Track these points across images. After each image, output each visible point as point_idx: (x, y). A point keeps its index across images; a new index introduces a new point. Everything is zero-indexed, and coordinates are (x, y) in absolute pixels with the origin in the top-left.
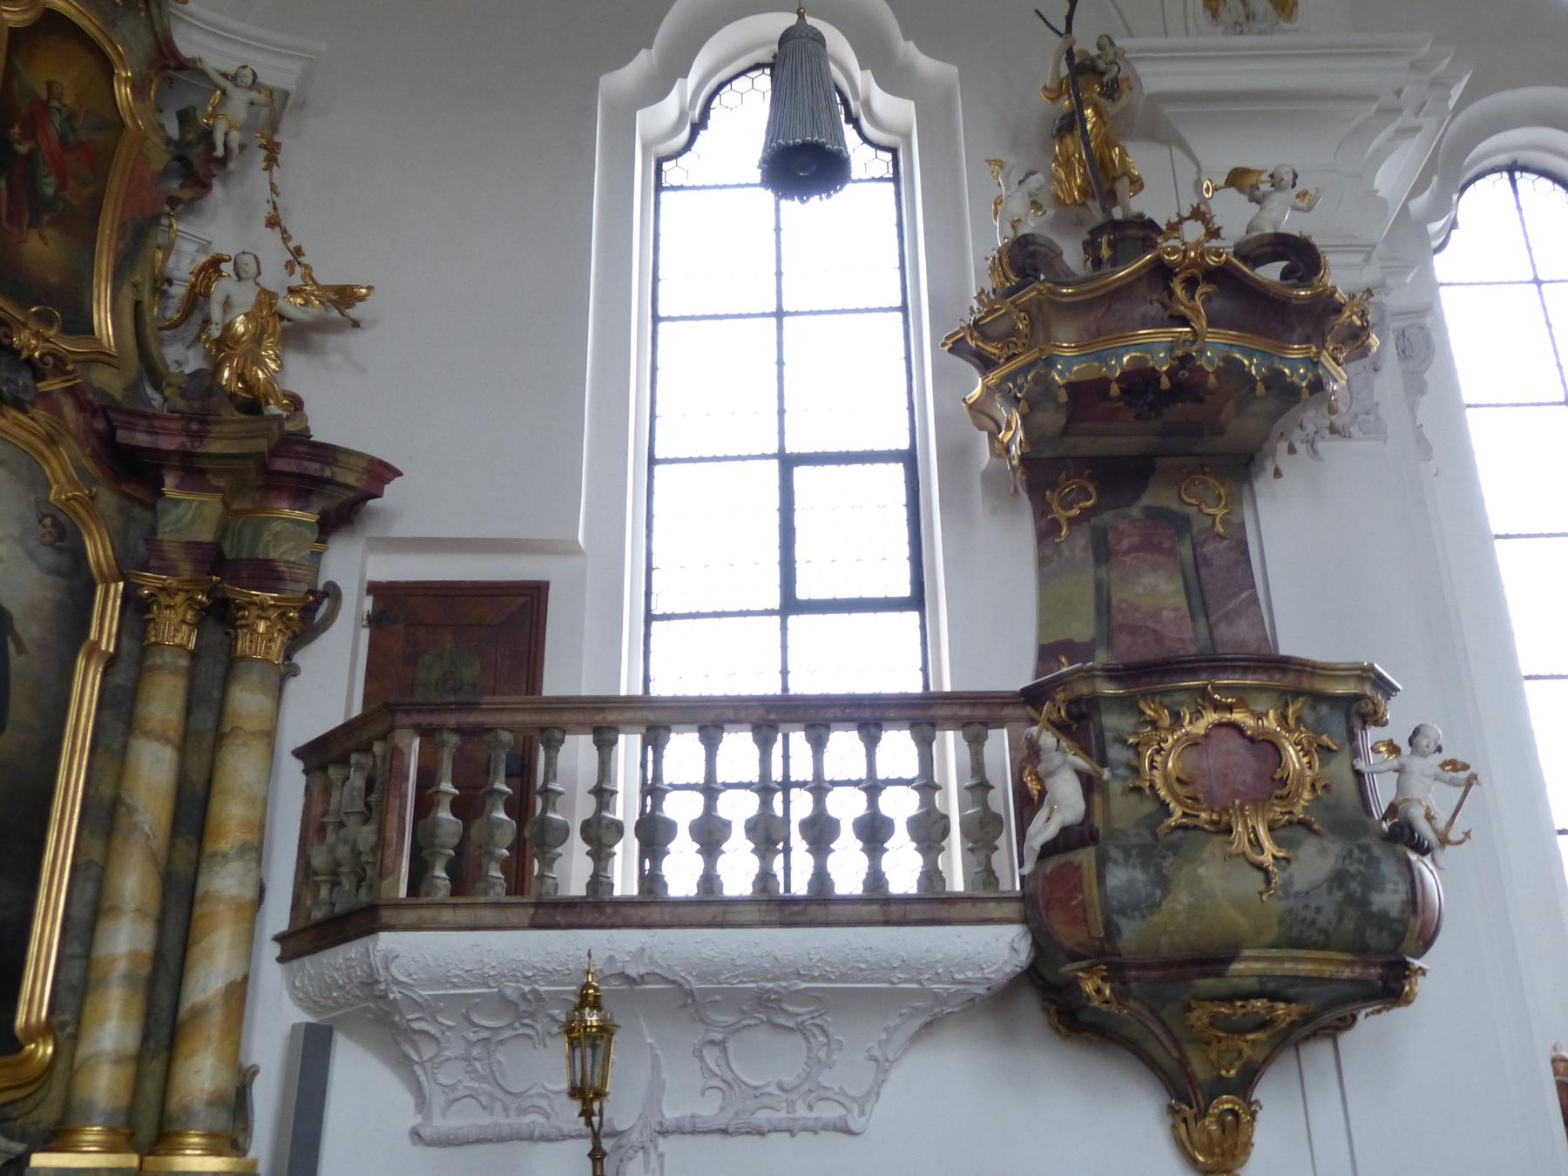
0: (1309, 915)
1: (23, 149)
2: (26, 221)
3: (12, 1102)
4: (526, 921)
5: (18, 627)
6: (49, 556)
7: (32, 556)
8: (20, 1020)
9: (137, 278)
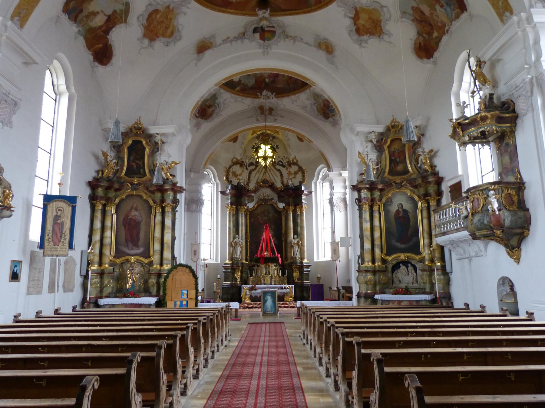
0: (477, 226)
1: (393, 158)
5: (409, 211)
6: (410, 202)
7: (408, 202)
8: (421, 251)
9: (413, 161)
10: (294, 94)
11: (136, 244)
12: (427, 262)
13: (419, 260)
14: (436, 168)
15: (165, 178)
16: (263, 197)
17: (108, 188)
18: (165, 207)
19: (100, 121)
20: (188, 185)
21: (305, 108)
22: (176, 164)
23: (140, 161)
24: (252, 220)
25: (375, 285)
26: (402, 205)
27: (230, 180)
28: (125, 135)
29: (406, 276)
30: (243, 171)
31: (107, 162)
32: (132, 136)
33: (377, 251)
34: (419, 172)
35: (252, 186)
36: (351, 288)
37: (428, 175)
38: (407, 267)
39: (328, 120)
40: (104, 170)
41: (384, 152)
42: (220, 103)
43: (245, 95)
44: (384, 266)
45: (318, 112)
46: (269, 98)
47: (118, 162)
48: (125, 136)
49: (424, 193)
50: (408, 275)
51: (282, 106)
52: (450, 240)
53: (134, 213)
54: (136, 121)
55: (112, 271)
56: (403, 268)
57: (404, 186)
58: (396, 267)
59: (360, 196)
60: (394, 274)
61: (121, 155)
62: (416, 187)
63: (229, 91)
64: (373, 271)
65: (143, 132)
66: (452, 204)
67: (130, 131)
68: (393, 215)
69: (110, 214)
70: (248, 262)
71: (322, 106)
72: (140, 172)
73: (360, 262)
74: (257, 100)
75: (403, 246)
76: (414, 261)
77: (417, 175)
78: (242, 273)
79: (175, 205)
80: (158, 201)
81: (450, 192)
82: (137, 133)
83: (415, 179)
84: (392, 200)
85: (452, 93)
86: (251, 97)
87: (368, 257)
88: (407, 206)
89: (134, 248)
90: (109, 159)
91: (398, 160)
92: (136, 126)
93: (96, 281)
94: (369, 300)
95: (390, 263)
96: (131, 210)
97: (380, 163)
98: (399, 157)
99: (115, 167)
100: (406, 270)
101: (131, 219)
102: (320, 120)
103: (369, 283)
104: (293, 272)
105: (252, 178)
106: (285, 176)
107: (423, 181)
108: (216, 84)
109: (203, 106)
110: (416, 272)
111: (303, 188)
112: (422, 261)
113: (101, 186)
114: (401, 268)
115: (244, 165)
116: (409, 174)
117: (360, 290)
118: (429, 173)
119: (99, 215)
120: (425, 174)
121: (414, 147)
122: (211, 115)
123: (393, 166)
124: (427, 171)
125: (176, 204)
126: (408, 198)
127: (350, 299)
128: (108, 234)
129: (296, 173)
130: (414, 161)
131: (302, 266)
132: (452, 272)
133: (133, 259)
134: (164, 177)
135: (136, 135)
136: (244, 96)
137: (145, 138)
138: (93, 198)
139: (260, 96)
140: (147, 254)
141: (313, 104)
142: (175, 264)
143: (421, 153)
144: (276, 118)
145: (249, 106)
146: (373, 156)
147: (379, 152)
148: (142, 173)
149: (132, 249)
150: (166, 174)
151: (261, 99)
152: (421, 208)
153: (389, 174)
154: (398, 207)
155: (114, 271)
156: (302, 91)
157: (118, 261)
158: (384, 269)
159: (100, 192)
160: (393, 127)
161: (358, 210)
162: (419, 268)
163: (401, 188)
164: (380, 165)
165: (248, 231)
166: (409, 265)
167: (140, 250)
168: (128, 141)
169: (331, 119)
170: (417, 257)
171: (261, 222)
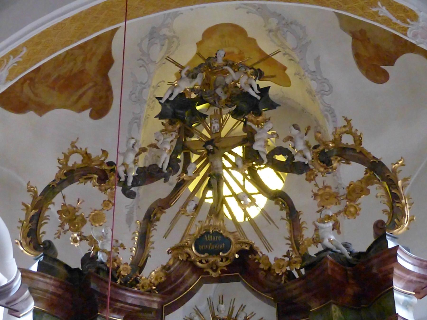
30: (107, 204)
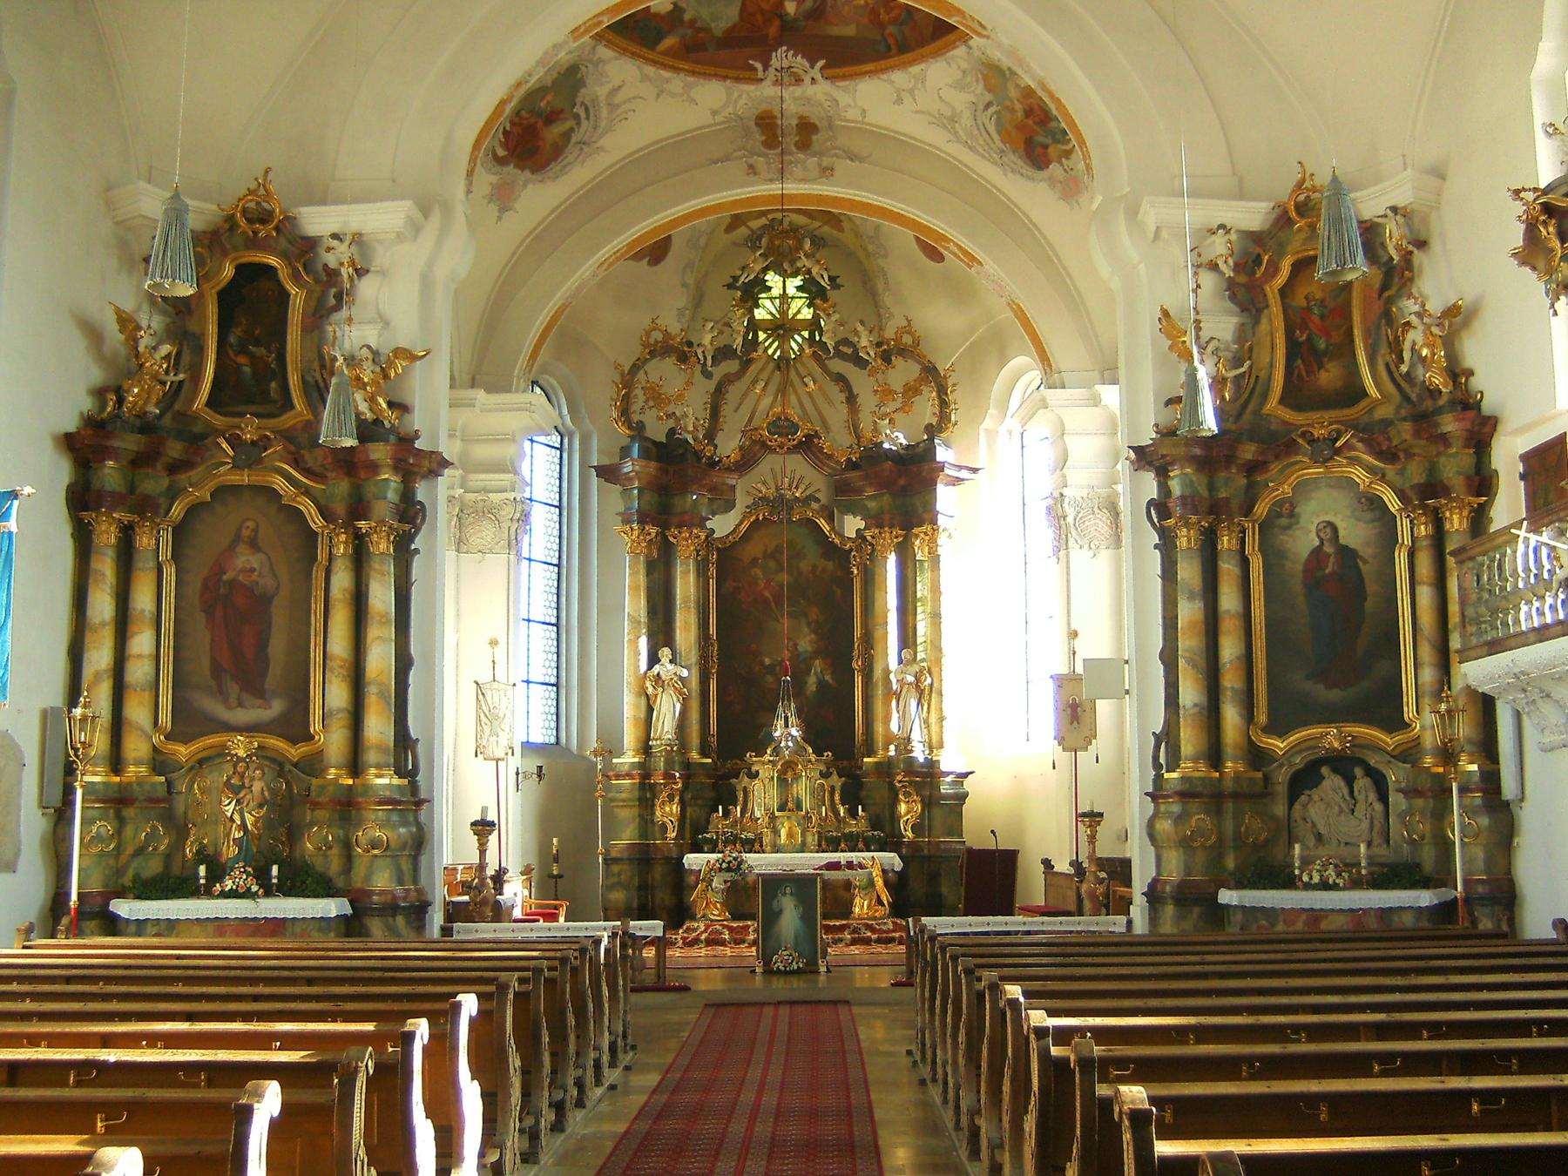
2: (1316, 368)
3: (1410, 748)
4: (1485, 652)
6: (1368, 516)
7: (1358, 519)
8: (1406, 716)
9: (1383, 352)
10: (903, 66)
11: (254, 686)
12: (1428, 761)
13: (1395, 753)
14: (1471, 378)
15: (369, 416)
16: (773, 490)
17: (141, 461)
18: (368, 534)
19: (109, 189)
20: (462, 440)
21: (948, 121)
22: (413, 358)
23: (270, 352)
24: (729, 585)
25: (1217, 851)
26: (1335, 529)
27: (636, 418)
28: (206, 242)
29: (1343, 817)
30: (689, 383)
31: (137, 355)
32: (235, 248)
33: (1231, 715)
34: (1406, 398)
35: (728, 446)
36: (1126, 864)
37: (1439, 411)
38: (1350, 781)
39: (1045, 174)
40: (125, 387)
41: (1266, 312)
42: (593, 101)
43: (698, 68)
44: (1259, 775)
45: (1005, 136)
46: (798, 81)
47: (179, 354)
48: (210, 248)
49: (1422, 481)
50: (1353, 811)
51: (852, 114)
52: (1516, 670)
53: (245, 559)
54: (253, 186)
55: (161, 792)
56: (1332, 782)
57: (1345, 451)
58: (1304, 780)
59: (1164, 489)
60: (1297, 806)
61: (193, 326)
62: (1389, 456)
63: (634, 55)
64: (1212, 796)
65: (277, 229)
66: (1520, 529)
67: (227, 226)
68: (1300, 567)
69: (152, 564)
70: (709, 761)
71: (1020, 115)
72: (265, 394)
73: (1162, 760)
74: (750, 88)
75: (1334, 695)
76: (1377, 758)
77: (1399, 407)
78: (682, 803)
79: (407, 527)
80: (340, 509)
81: (1523, 477)
82: (255, 233)
83: (1387, 423)
84: (1296, 510)
85: (1534, 75)
86: (725, 78)
87: (1190, 738)
88: (1355, 533)
89: (248, 699)
90: (145, 342)
91: (1322, 344)
92: (252, 205)
93: (102, 830)
94: (1196, 910)
95: (1281, 765)
96: (233, 546)
97: (1250, 358)
98: (1326, 333)
99: (167, 372)
100: (1346, 791)
101: (233, 583)
102: (1013, 171)
103: (1195, 844)
104: (895, 802)
105: (727, 410)
106: (867, 401)
107: (1417, 434)
108: (577, 29)
109: (524, 114)
110: (1383, 797)
111: (942, 454)
112: (1409, 754)
113: (113, 453)
114: (1326, 784)
115: (693, 359)
116: (1363, 404)
117: (1159, 873)
118: (1441, 402)
119: (105, 566)
120: (1428, 404)
121: (1386, 294)
122: (558, 151)
123: (1302, 366)
124: (1434, 393)
125: (412, 521)
126: (1360, 502)
127: (1124, 905)
128: (141, 643)
129: (911, 391)
130: (1384, 349)
131: (930, 772)
132: (1522, 800)
133: (240, 746)
134: (363, 413)
135: (254, 243)
136: (693, 73)
137: (284, 256)
138: (82, 500)
139: (760, 74)
140: (295, 726)
141: (981, 107)
142: (410, 767)
143: (1414, 320)
144: (826, 161)
145: (714, 113)
146: (1223, 325)
147: (1244, 309)
148: (273, 395)
149: (241, 705)
150: (371, 400)
151: (764, 83)
152: (1408, 541)
153: (1283, 401)
154: (1319, 536)
155: (169, 792)
156: (936, 54)
157: (182, 751)
158: (1259, 788)
159: (110, 473)
160: (1303, 208)
161: (1156, 547)
162: (1397, 781)
163: (1332, 458)
164: (1248, 363)
165: (713, 630)
166: (1358, 771)
167: (270, 708)
168: (220, 269)
169: (1055, 169)
170: (1389, 741)
171: (767, 594)
